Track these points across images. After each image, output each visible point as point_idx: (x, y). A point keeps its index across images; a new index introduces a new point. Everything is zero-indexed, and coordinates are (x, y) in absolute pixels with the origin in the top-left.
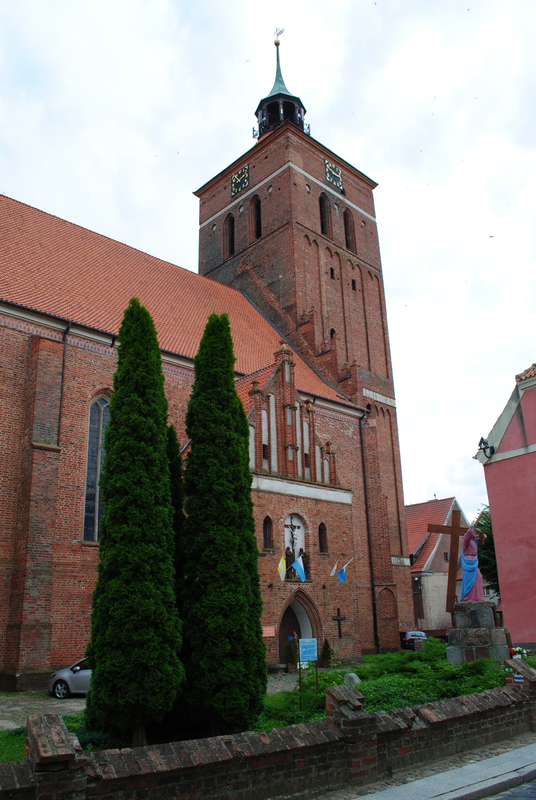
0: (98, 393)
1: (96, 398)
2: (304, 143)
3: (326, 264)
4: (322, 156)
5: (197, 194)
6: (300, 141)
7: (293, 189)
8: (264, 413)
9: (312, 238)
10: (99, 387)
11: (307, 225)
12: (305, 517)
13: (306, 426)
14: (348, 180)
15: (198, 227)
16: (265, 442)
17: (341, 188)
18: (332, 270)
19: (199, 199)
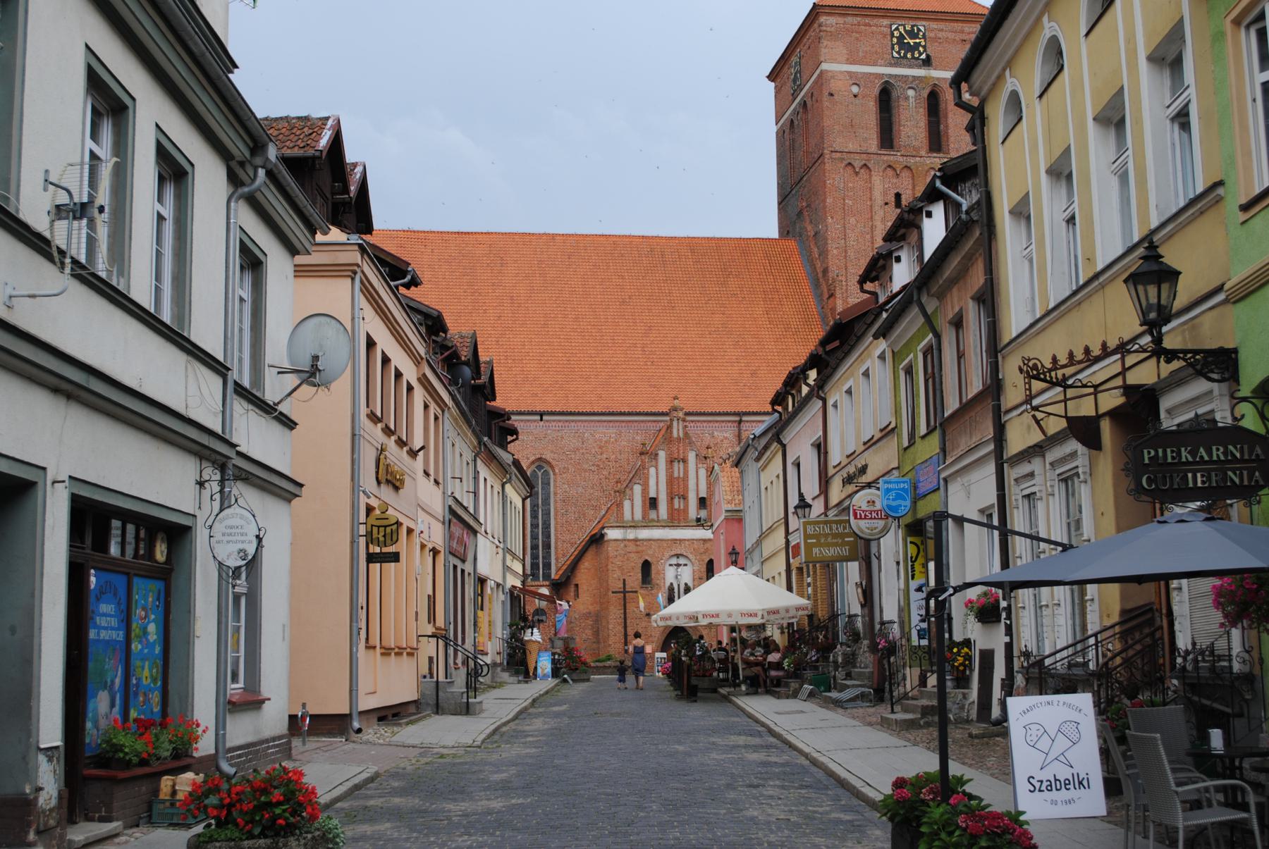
0: (533, 462)
1: (533, 467)
2: (849, 19)
3: (885, 193)
4: (886, 22)
5: (772, 76)
6: (841, 20)
7: (826, 104)
8: (652, 470)
9: (857, 164)
10: (532, 458)
11: (851, 147)
12: (690, 556)
13: (703, 473)
14: (940, 35)
15: (774, 129)
16: (652, 494)
17: (923, 56)
18: (898, 196)
19: (773, 84)
